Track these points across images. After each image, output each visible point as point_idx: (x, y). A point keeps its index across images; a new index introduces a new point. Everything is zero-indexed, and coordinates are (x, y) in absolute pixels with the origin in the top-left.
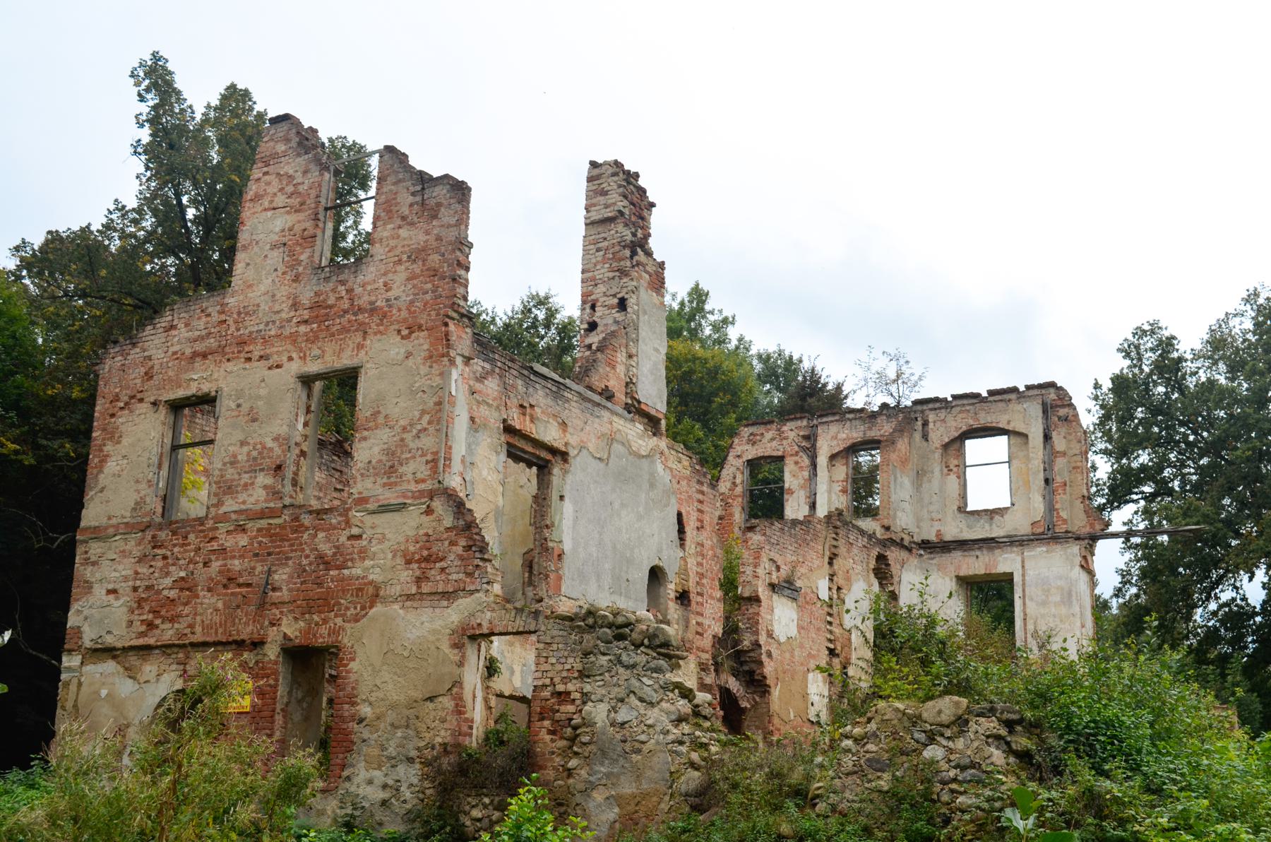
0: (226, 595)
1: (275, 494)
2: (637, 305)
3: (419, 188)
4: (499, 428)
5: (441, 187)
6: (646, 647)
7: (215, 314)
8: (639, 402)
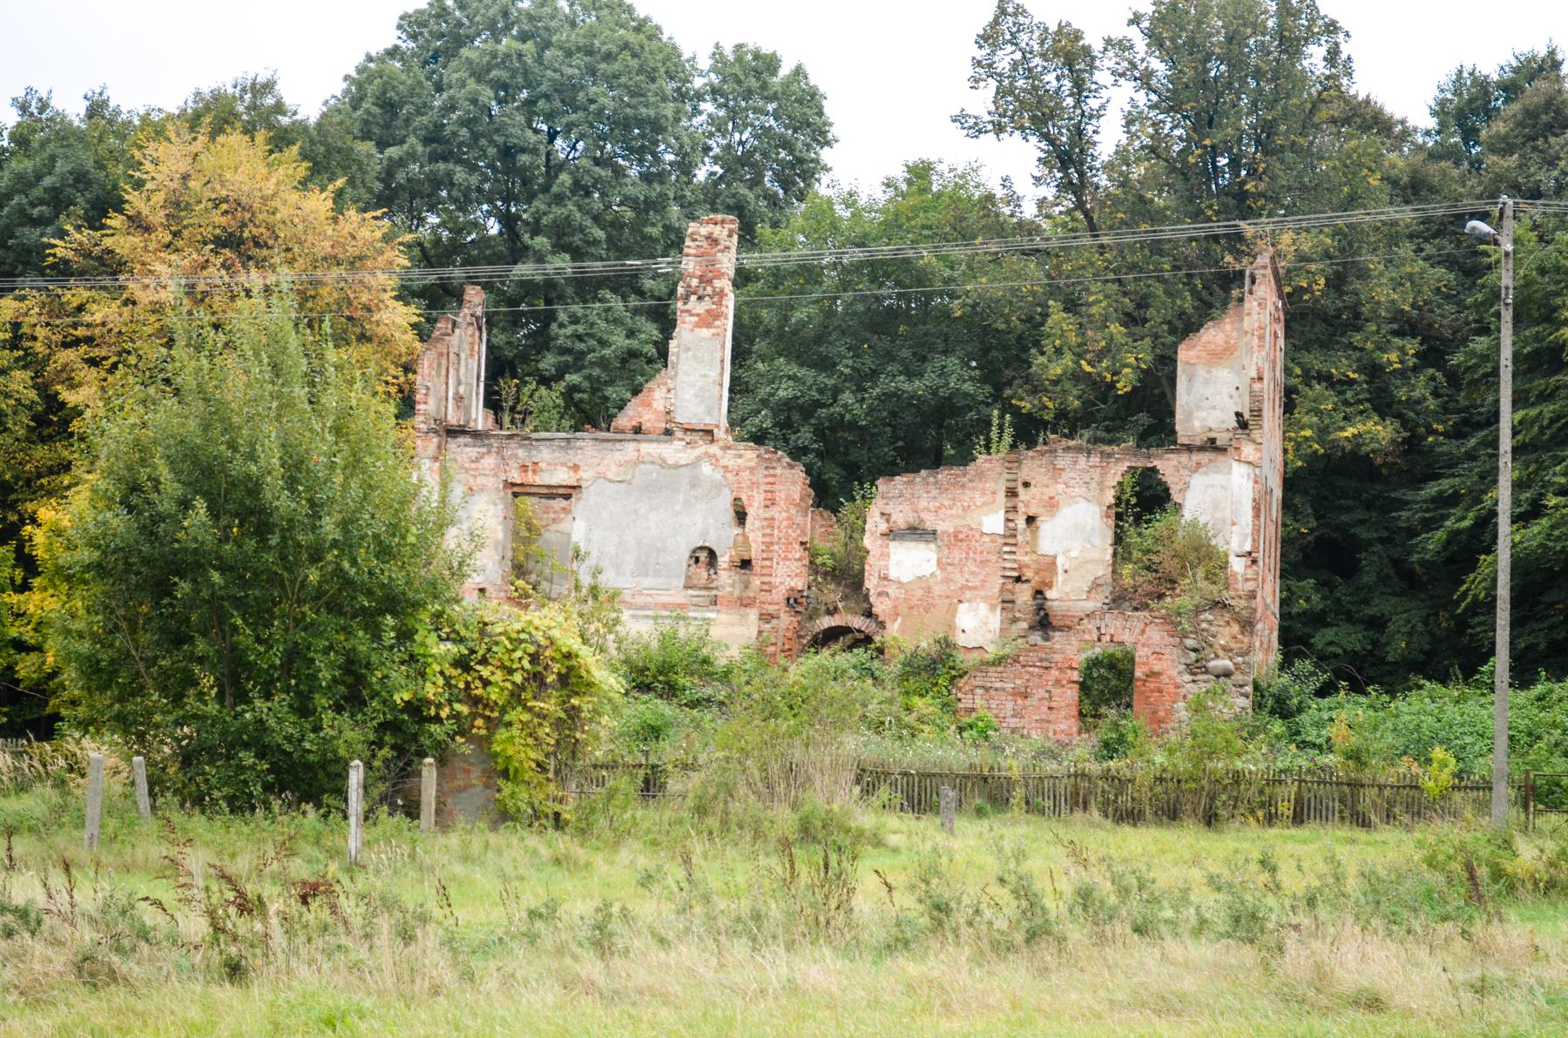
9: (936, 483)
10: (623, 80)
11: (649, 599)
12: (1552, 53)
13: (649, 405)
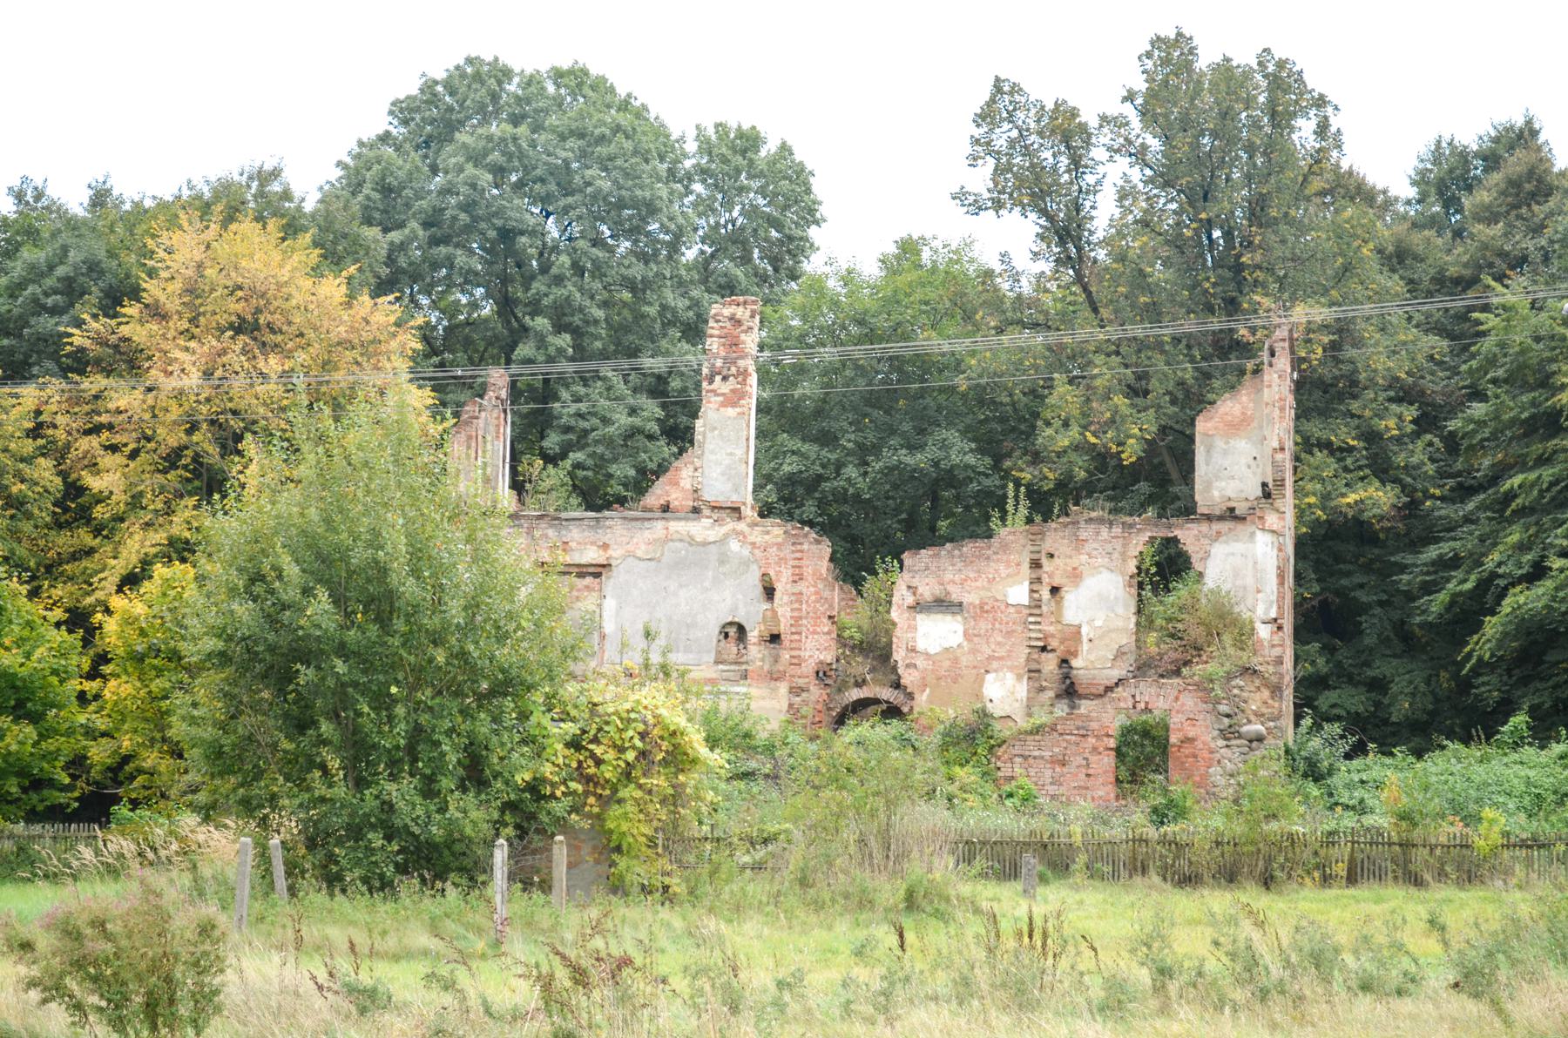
9: (961, 556)
10: (619, 162)
12: (1529, 122)
13: (677, 484)
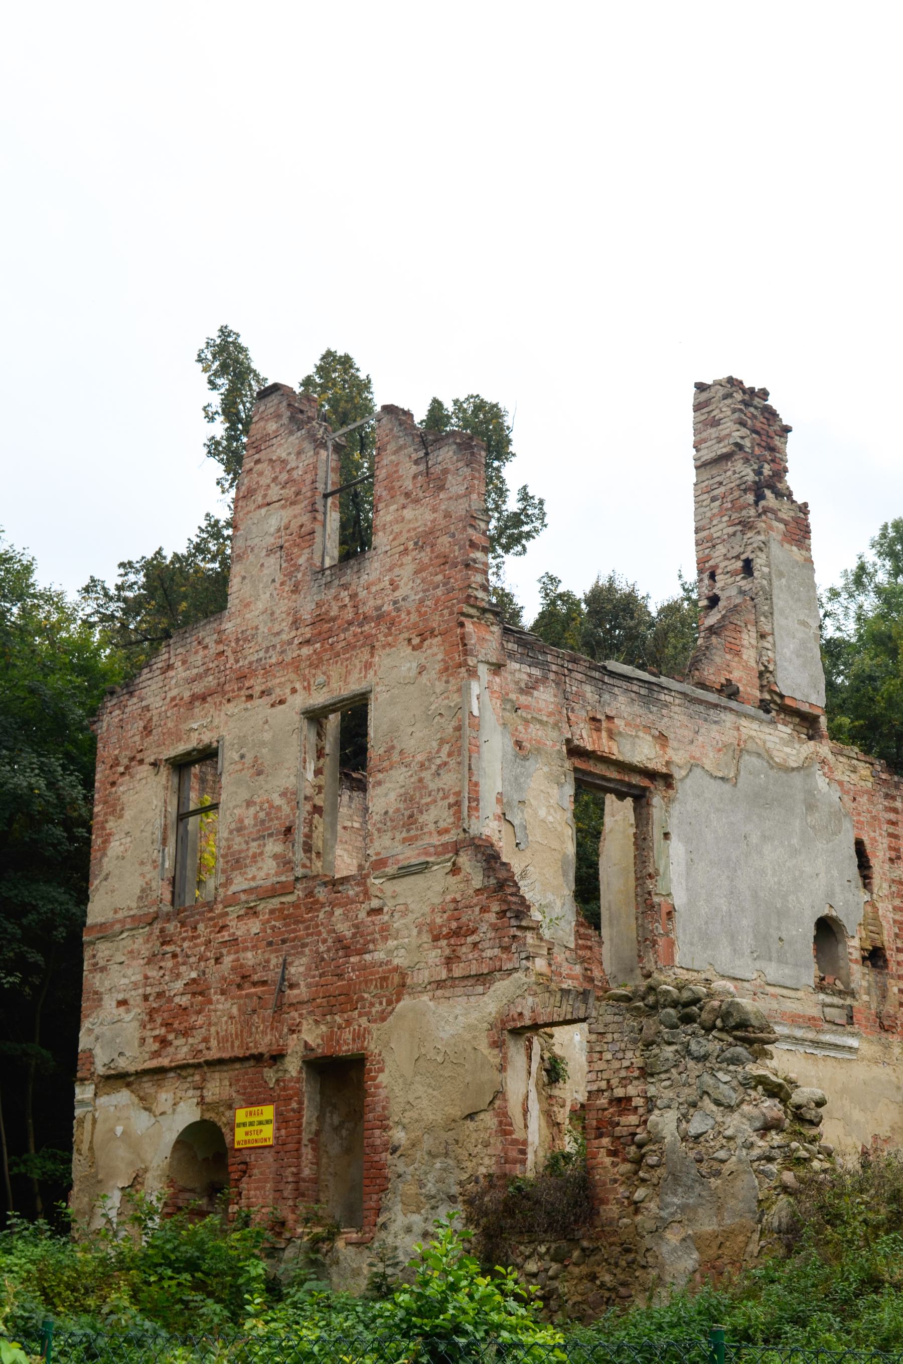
0: (240, 997)
1: (286, 863)
2: (768, 566)
3: (421, 454)
4: (559, 752)
5: (446, 449)
6: (721, 1030)
7: (212, 645)
8: (782, 697)
11: (775, 1006)
